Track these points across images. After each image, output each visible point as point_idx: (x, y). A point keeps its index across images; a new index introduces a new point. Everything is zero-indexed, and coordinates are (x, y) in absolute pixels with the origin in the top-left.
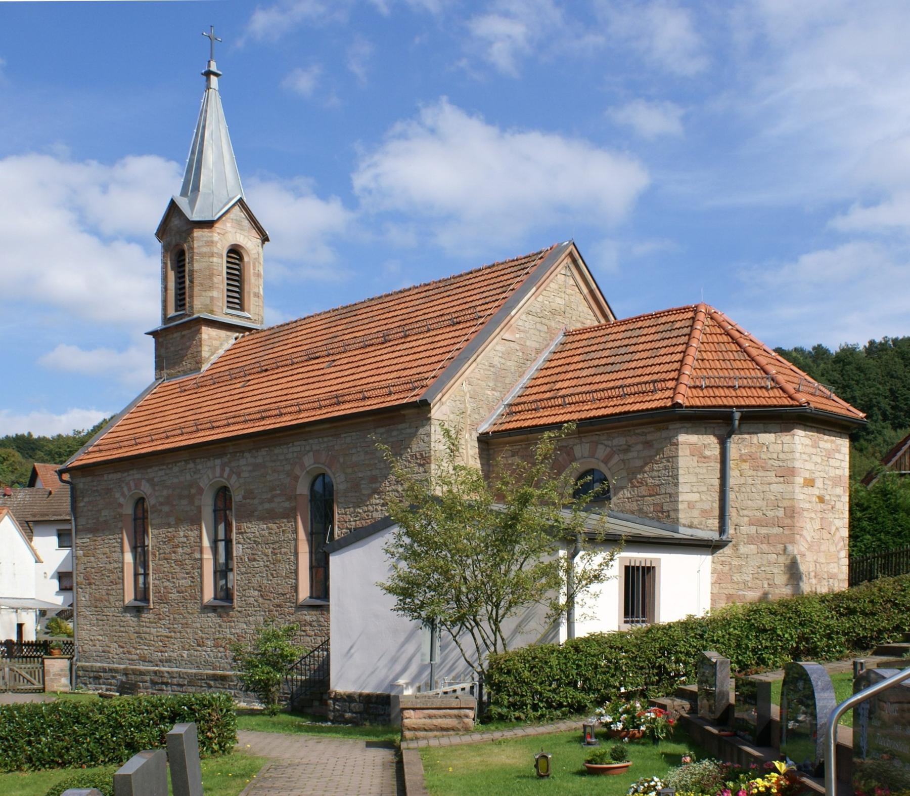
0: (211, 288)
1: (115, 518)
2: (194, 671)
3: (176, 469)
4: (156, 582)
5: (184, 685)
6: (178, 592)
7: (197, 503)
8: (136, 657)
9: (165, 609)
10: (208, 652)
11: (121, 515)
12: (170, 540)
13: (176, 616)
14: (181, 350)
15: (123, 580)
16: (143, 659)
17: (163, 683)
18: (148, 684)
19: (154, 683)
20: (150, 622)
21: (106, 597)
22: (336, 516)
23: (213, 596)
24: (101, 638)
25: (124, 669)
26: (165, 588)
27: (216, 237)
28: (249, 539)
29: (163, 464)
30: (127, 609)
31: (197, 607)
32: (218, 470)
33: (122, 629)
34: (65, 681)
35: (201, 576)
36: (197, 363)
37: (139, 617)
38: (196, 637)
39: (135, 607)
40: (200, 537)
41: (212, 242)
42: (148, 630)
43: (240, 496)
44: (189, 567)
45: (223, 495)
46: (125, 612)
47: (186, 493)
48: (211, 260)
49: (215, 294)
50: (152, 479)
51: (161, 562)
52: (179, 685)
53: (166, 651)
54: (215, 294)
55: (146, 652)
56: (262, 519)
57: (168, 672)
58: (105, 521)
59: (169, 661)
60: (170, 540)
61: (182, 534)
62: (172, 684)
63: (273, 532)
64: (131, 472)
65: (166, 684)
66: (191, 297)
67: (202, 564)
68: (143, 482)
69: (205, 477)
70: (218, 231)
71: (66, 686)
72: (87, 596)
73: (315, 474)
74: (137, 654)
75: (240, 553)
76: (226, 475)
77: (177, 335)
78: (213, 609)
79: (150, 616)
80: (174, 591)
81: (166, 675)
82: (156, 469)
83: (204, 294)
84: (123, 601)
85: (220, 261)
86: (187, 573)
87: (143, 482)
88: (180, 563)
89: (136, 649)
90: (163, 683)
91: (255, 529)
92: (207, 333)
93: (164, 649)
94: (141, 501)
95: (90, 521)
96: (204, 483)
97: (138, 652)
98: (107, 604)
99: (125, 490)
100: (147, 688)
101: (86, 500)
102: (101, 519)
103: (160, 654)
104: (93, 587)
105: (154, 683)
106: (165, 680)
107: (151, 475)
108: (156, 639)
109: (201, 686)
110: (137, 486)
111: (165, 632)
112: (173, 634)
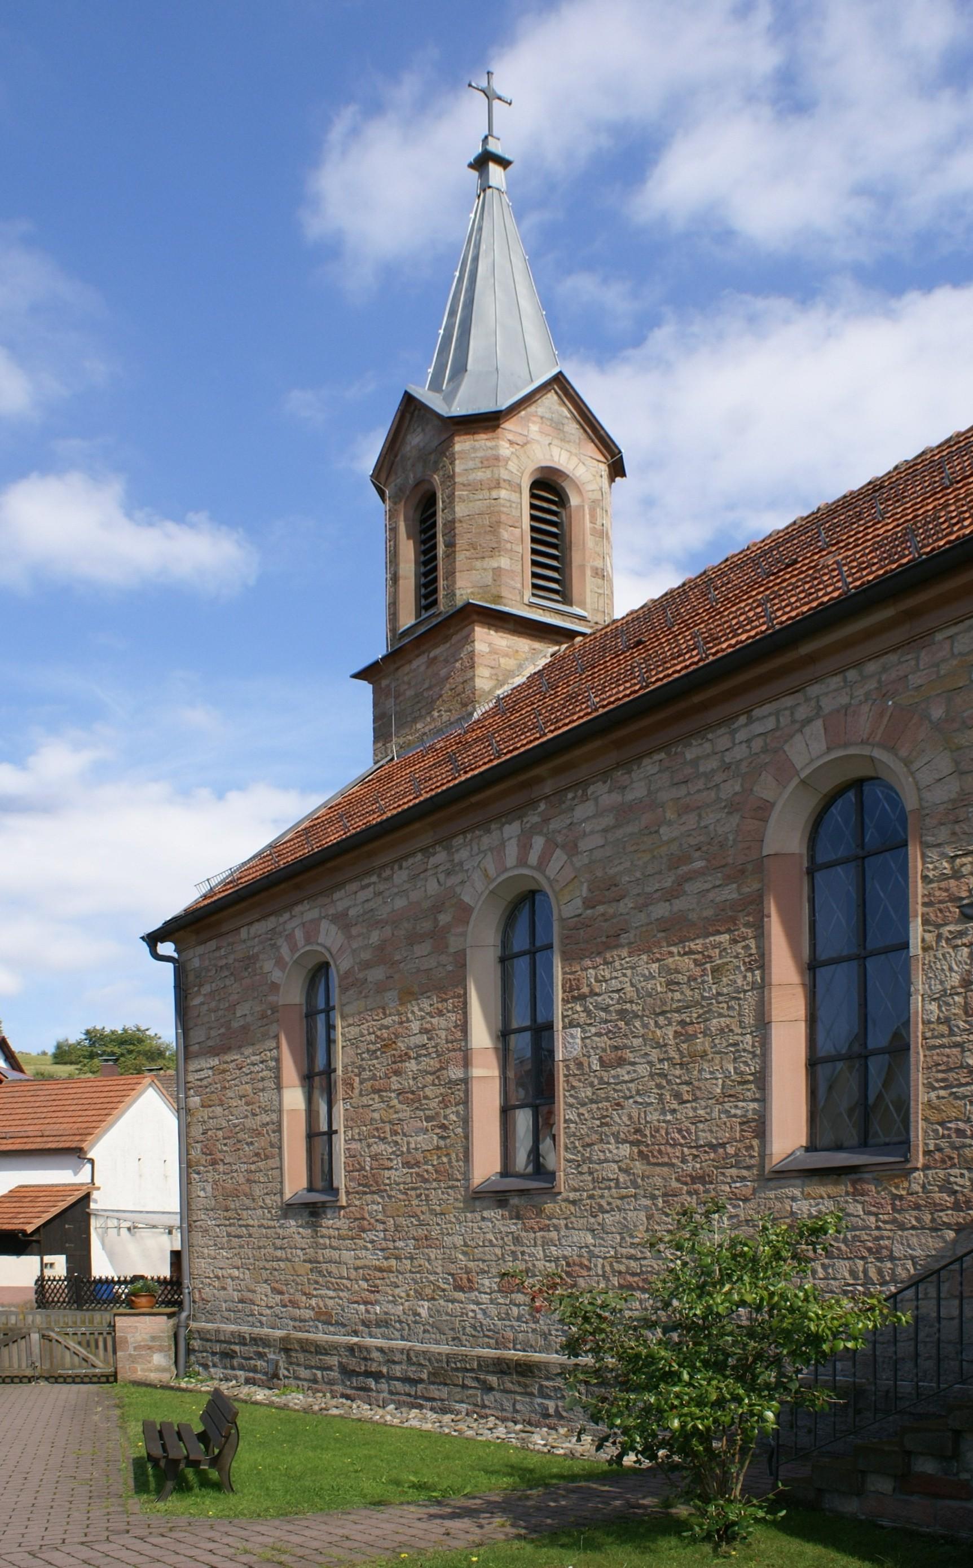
0: (495, 551)
1: (264, 1016)
2: (444, 1349)
3: (401, 876)
4: (355, 1145)
5: (421, 1381)
6: (407, 1164)
7: (454, 944)
8: (308, 1314)
9: (374, 1206)
10: (484, 1305)
11: (274, 1009)
12: (387, 1045)
13: (401, 1220)
14: (429, 688)
15: (280, 1148)
16: (325, 1318)
17: (368, 1374)
18: (335, 1374)
19: (347, 1372)
20: (340, 1238)
21: (246, 1188)
22: (919, 890)
23: (498, 1169)
24: (236, 1273)
25: (283, 1339)
26: (374, 1157)
27: (505, 449)
28: (605, 1010)
29: (368, 873)
30: (289, 1209)
31: (455, 1198)
32: (512, 851)
33: (279, 1253)
34: (159, 1359)
35: (466, 1121)
36: (465, 705)
37: (315, 1226)
38: (452, 1268)
39: (306, 1205)
40: (464, 1028)
41: (497, 458)
42: (335, 1254)
43: (579, 902)
44: (433, 1104)
45: (524, 904)
46: (285, 1216)
47: (427, 925)
48: (494, 494)
49: (504, 562)
50: (345, 914)
51: (365, 1100)
52: (406, 1380)
53: (377, 1302)
54: (504, 562)
55: (330, 1303)
56: (643, 947)
57: (381, 1350)
58: (243, 1027)
59: (383, 1323)
60: (387, 1045)
61: (415, 1026)
62: (390, 1378)
63: (681, 978)
64: (297, 909)
65: (377, 1376)
66: (451, 574)
67: (467, 1092)
68: (324, 924)
69: (477, 876)
70: (510, 437)
71: (164, 1370)
72: (209, 1189)
73: (827, 786)
74: (311, 1308)
75: (577, 1050)
76: (533, 858)
77: (419, 663)
78: (498, 1198)
79: (339, 1224)
80: (397, 1162)
81: (375, 1355)
82: (354, 886)
83: (478, 564)
84: (281, 1193)
85: (514, 497)
86: (428, 1119)
87: (324, 924)
88: (412, 1098)
89: (309, 1296)
90: (368, 1374)
91: (624, 976)
92: (485, 640)
93: (372, 1297)
94: (320, 972)
95: (213, 1033)
96: (474, 892)
97: (313, 1302)
98: (248, 1202)
99: (285, 951)
100: (331, 1383)
101: (206, 989)
102: (235, 1025)
103: (362, 1307)
104: (221, 1168)
105: (347, 1372)
106: (374, 1367)
107: (340, 906)
108: (353, 1274)
109: (464, 1387)
110: (311, 933)
111: (372, 1258)
112: (393, 1262)
